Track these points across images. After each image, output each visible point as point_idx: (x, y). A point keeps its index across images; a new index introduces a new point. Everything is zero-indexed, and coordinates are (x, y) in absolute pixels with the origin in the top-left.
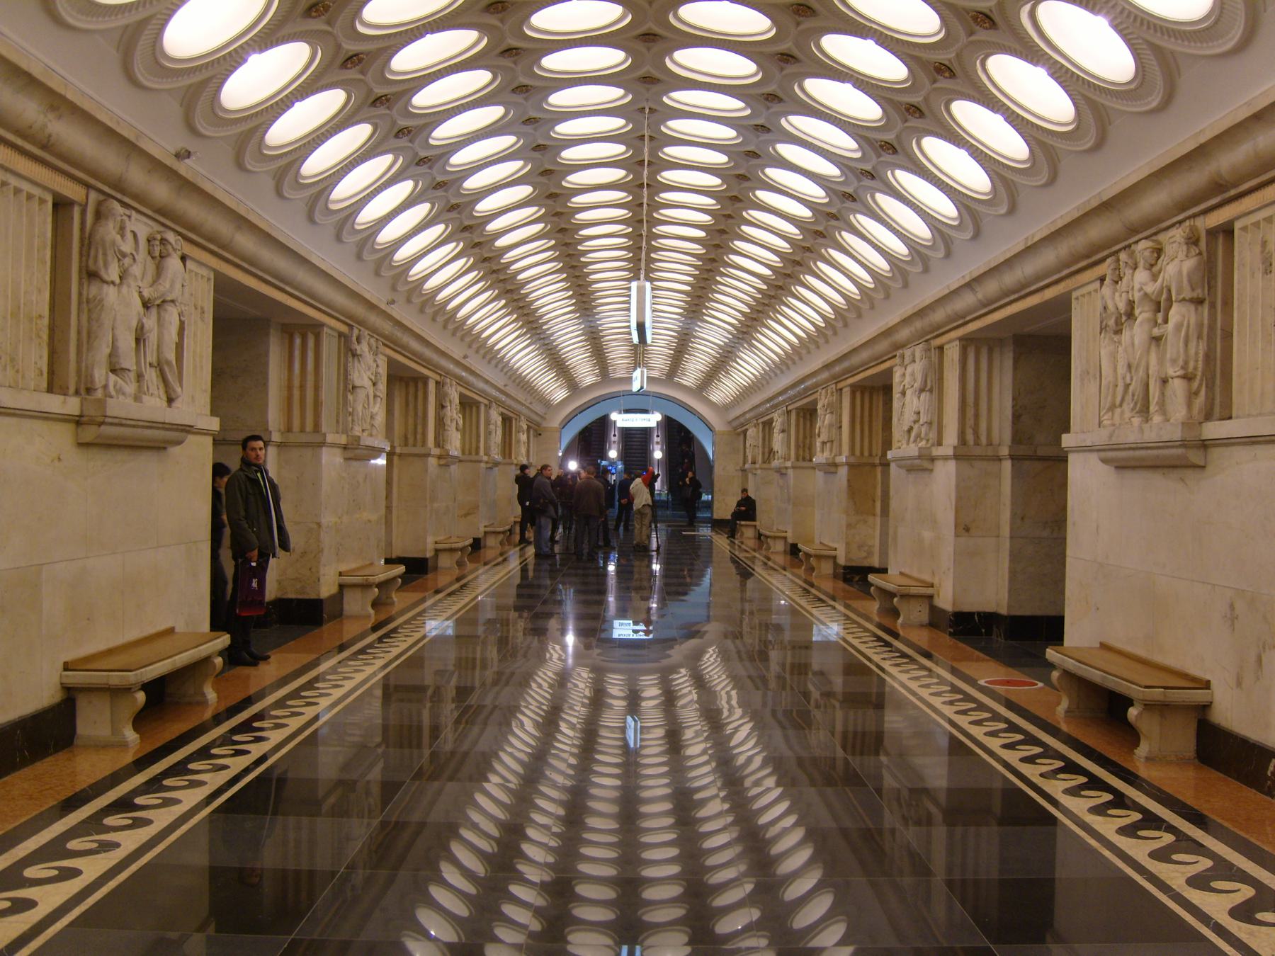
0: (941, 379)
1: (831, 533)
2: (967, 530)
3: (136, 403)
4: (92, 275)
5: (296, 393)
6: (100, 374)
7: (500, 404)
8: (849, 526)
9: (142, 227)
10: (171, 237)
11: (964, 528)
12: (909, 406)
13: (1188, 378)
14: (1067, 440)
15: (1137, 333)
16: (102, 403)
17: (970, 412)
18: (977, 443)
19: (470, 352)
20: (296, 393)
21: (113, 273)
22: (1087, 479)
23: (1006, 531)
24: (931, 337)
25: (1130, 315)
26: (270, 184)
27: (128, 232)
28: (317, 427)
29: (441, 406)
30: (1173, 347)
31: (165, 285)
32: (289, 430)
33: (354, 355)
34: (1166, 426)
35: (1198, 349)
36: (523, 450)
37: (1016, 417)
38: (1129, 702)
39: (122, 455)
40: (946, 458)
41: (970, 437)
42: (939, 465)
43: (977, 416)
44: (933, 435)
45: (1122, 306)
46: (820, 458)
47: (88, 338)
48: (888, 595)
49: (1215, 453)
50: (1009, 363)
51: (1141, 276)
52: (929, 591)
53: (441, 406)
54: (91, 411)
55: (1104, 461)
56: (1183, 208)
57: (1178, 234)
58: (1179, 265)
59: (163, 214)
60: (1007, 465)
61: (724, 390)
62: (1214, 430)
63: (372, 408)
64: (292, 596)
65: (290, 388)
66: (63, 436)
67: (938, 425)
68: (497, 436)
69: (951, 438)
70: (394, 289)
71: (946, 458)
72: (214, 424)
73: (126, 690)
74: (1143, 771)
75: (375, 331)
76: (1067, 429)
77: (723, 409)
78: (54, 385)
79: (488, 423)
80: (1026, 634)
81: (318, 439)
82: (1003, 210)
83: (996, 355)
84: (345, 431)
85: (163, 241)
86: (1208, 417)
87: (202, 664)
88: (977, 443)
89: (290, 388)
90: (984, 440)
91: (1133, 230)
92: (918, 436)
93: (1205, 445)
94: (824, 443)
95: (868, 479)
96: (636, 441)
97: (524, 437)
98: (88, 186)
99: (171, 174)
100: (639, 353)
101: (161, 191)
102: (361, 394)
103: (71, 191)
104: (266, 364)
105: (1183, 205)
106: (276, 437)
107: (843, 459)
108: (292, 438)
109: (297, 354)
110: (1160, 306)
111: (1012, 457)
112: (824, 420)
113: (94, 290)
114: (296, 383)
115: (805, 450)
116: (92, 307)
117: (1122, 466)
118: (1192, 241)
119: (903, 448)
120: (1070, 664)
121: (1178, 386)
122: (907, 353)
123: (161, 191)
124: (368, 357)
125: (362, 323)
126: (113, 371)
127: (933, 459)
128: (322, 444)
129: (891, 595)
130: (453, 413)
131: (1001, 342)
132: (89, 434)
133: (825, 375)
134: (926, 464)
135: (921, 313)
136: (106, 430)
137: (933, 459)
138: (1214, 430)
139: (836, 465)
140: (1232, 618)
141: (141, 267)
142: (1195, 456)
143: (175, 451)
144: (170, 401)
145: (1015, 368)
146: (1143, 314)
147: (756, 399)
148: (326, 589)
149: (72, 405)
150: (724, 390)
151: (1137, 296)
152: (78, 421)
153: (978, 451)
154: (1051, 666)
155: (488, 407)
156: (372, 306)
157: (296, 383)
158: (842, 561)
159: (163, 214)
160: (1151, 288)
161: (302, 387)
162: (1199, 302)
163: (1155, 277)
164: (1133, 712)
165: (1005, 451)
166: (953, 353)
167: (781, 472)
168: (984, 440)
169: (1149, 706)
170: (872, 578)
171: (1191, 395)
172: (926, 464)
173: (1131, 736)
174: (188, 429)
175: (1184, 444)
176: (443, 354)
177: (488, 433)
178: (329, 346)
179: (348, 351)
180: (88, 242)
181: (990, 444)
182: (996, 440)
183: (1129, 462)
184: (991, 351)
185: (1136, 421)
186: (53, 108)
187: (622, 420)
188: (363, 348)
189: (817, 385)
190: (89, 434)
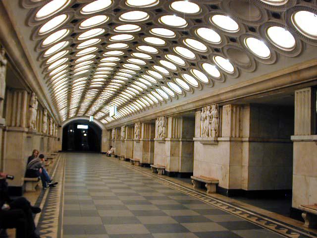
2: (173, 155)
8: (143, 154)
11: (172, 155)
13: (215, 130)
14: (194, 139)
15: (207, 122)
17: (174, 131)
18: (175, 138)
21: (33, 106)
22: (198, 146)
23: (180, 155)
25: (206, 118)
30: (213, 125)
35: (217, 126)
37: (183, 133)
38: (205, 183)
41: (173, 137)
45: (205, 117)
49: (219, 143)
51: (208, 112)
54: (30, 131)
58: (214, 112)
60: (181, 142)
67: (166, 133)
71: (168, 141)
75: (48, 111)
77: (104, 125)
80: (186, 176)
82: (184, 96)
86: (219, 137)
88: (175, 138)
92: (162, 136)
93: (218, 141)
94: (137, 136)
95: (149, 145)
102: (45, 124)
110: (211, 117)
111: (182, 141)
112: (136, 130)
113: (30, 109)
118: (216, 108)
120: (195, 178)
121: (214, 132)
129: (156, 169)
137: (165, 141)
138: (219, 139)
139: (140, 140)
140: (222, 169)
142: (216, 143)
153: (174, 139)
154: (193, 179)
158: (141, 162)
160: (210, 115)
162: (217, 118)
164: (206, 185)
165: (181, 140)
169: (209, 184)
170: (151, 165)
171: (216, 133)
173: (206, 189)
181: (177, 138)
183: (205, 143)
185: (207, 136)
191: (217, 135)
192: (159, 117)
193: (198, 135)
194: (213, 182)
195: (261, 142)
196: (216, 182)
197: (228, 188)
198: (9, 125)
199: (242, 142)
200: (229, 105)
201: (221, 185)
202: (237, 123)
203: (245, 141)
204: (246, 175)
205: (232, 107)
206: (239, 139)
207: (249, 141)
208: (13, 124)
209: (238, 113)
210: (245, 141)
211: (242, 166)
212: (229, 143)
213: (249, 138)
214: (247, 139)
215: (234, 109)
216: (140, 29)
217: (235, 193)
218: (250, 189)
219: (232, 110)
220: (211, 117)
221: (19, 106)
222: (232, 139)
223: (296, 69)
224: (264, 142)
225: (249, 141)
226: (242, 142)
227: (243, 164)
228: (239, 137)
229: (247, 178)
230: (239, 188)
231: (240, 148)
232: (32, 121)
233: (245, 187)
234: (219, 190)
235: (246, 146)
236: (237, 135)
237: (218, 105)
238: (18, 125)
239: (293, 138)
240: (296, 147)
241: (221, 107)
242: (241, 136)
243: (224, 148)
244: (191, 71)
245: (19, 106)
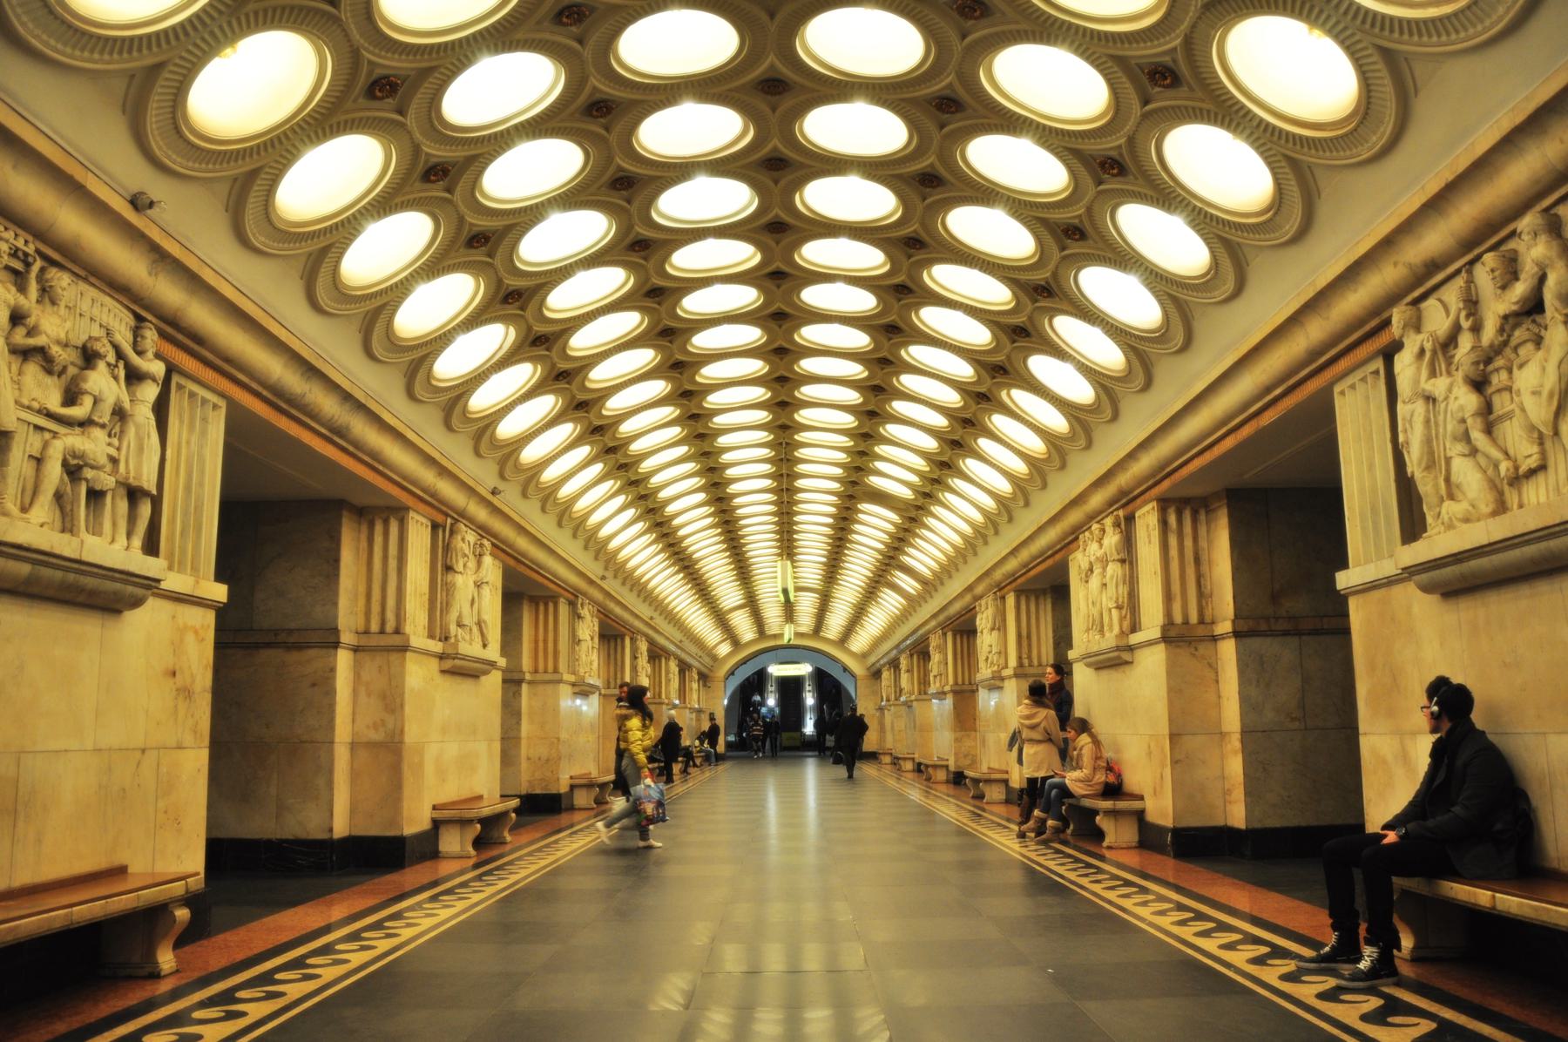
0: (1004, 620)
1: (942, 746)
3: (470, 647)
4: (449, 568)
5: (541, 644)
6: (453, 628)
7: (677, 657)
8: (957, 740)
9: (471, 537)
10: (486, 542)
12: (986, 641)
13: (1119, 608)
14: (1071, 655)
15: (1095, 581)
16: (456, 645)
17: (1025, 643)
19: (655, 615)
20: (541, 644)
21: (460, 567)
24: (1000, 589)
25: (1091, 570)
26: (539, 504)
27: (467, 538)
28: (556, 671)
29: (634, 657)
30: (1111, 590)
31: (483, 572)
32: (536, 671)
33: (579, 617)
34: (1110, 640)
36: (695, 696)
39: (458, 679)
40: (1010, 677)
41: (1026, 662)
42: (1007, 684)
43: (1030, 645)
44: (1002, 661)
46: (932, 689)
47: (447, 606)
48: (976, 781)
50: (1049, 606)
52: (1005, 776)
53: (634, 657)
54: (450, 651)
55: (1088, 665)
56: (1111, 505)
57: (1108, 521)
58: (1112, 539)
59: (483, 530)
61: (860, 642)
62: (1135, 639)
63: (590, 660)
64: (538, 791)
65: (536, 642)
66: (434, 664)
67: (1003, 653)
68: (675, 684)
69: (1013, 662)
70: (606, 569)
72: (502, 662)
73: (470, 822)
74: (1108, 854)
75: (593, 601)
76: (1070, 646)
77: (864, 656)
78: (431, 636)
79: (667, 672)
81: (556, 677)
83: (1041, 600)
84: (574, 673)
85: (482, 545)
87: (503, 815)
89: (536, 642)
90: (1035, 662)
91: (1091, 518)
93: (1131, 649)
96: (790, 688)
97: (695, 686)
98: (447, 515)
99: (489, 504)
100: (789, 610)
101: (481, 514)
102: (584, 646)
103: (440, 518)
104: (520, 625)
105: (1111, 503)
106: (528, 677)
107: (947, 688)
108: (539, 677)
109: (541, 617)
112: (936, 657)
113: (450, 577)
114: (541, 637)
115: (924, 682)
116: (449, 589)
117: (1097, 669)
118: (1117, 525)
119: (984, 672)
121: (1115, 613)
122: (983, 602)
123: (481, 514)
124: (588, 617)
125: (585, 594)
126: (460, 625)
127: (1002, 679)
128: (560, 681)
130: (643, 661)
131: (1044, 592)
132: (448, 664)
133: (933, 623)
134: (998, 683)
135: (987, 573)
136: (457, 662)
138: (1135, 639)
139: (944, 693)
141: (472, 564)
143: (483, 678)
144: (485, 646)
145: (1054, 610)
146: (1097, 571)
147: (887, 646)
148: (563, 788)
149: (437, 647)
150: (860, 642)
151: (1093, 559)
152: (442, 657)
155: (667, 659)
156: (591, 582)
157: (541, 637)
158: (952, 768)
159: (483, 530)
160: (1100, 553)
161: (545, 641)
162: (1123, 561)
163: (1101, 546)
166: (1011, 600)
167: (908, 705)
168: (1035, 662)
171: (1122, 619)
172: (998, 683)
173: (1099, 835)
174: (492, 664)
175: (1118, 648)
176: (637, 616)
177: (668, 681)
178: (564, 609)
179: (576, 616)
180: (447, 548)
182: (1044, 661)
184: (1037, 598)
186: (440, 474)
187: (776, 670)
188: (585, 612)
189: (929, 632)
190: (448, 664)
191: (1126, 624)
192: (981, 597)
193: (1083, 641)
194: (994, 776)
195: (1286, 633)
196: (1136, 805)
197: (1168, 822)
198: (361, 629)
199: (1215, 639)
200: (1150, 506)
201: (1153, 817)
202: (1187, 572)
203: (1223, 637)
204: (1235, 766)
205: (1163, 511)
206: (1201, 631)
207: (1237, 634)
208: (374, 627)
209: (1188, 529)
210: (1223, 637)
211: (1223, 735)
212: (1162, 646)
213: (1233, 622)
214: (1225, 627)
215: (1172, 519)
216: (758, 258)
217: (1199, 846)
218: (1257, 825)
219: (1164, 523)
220: (1104, 562)
221: (393, 563)
222: (1173, 633)
223: (1311, 294)
224: (1298, 633)
225: (1237, 634)
226: (1215, 639)
227: (1224, 729)
228: (1201, 621)
229: (1241, 778)
230: (1220, 823)
231: (1210, 665)
232: (460, 616)
233: (1237, 816)
234: (1149, 837)
235: (1228, 651)
236: (1194, 619)
237: (1121, 513)
238: (390, 627)
239: (1343, 580)
240: (1358, 614)
241: (1130, 519)
242: (1208, 619)
243: (1152, 663)
244: (1004, 394)
245: (393, 563)
